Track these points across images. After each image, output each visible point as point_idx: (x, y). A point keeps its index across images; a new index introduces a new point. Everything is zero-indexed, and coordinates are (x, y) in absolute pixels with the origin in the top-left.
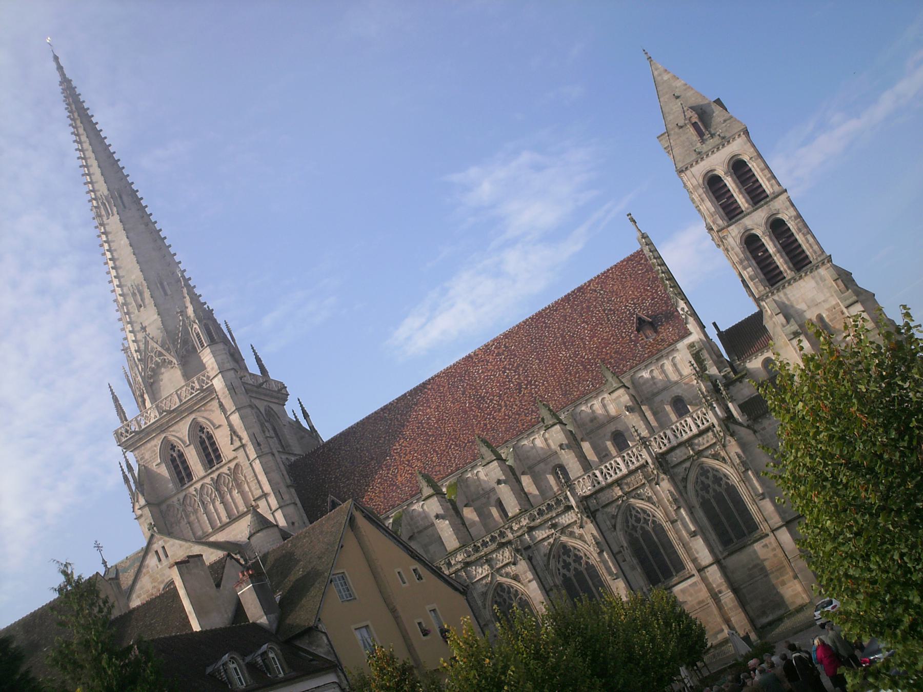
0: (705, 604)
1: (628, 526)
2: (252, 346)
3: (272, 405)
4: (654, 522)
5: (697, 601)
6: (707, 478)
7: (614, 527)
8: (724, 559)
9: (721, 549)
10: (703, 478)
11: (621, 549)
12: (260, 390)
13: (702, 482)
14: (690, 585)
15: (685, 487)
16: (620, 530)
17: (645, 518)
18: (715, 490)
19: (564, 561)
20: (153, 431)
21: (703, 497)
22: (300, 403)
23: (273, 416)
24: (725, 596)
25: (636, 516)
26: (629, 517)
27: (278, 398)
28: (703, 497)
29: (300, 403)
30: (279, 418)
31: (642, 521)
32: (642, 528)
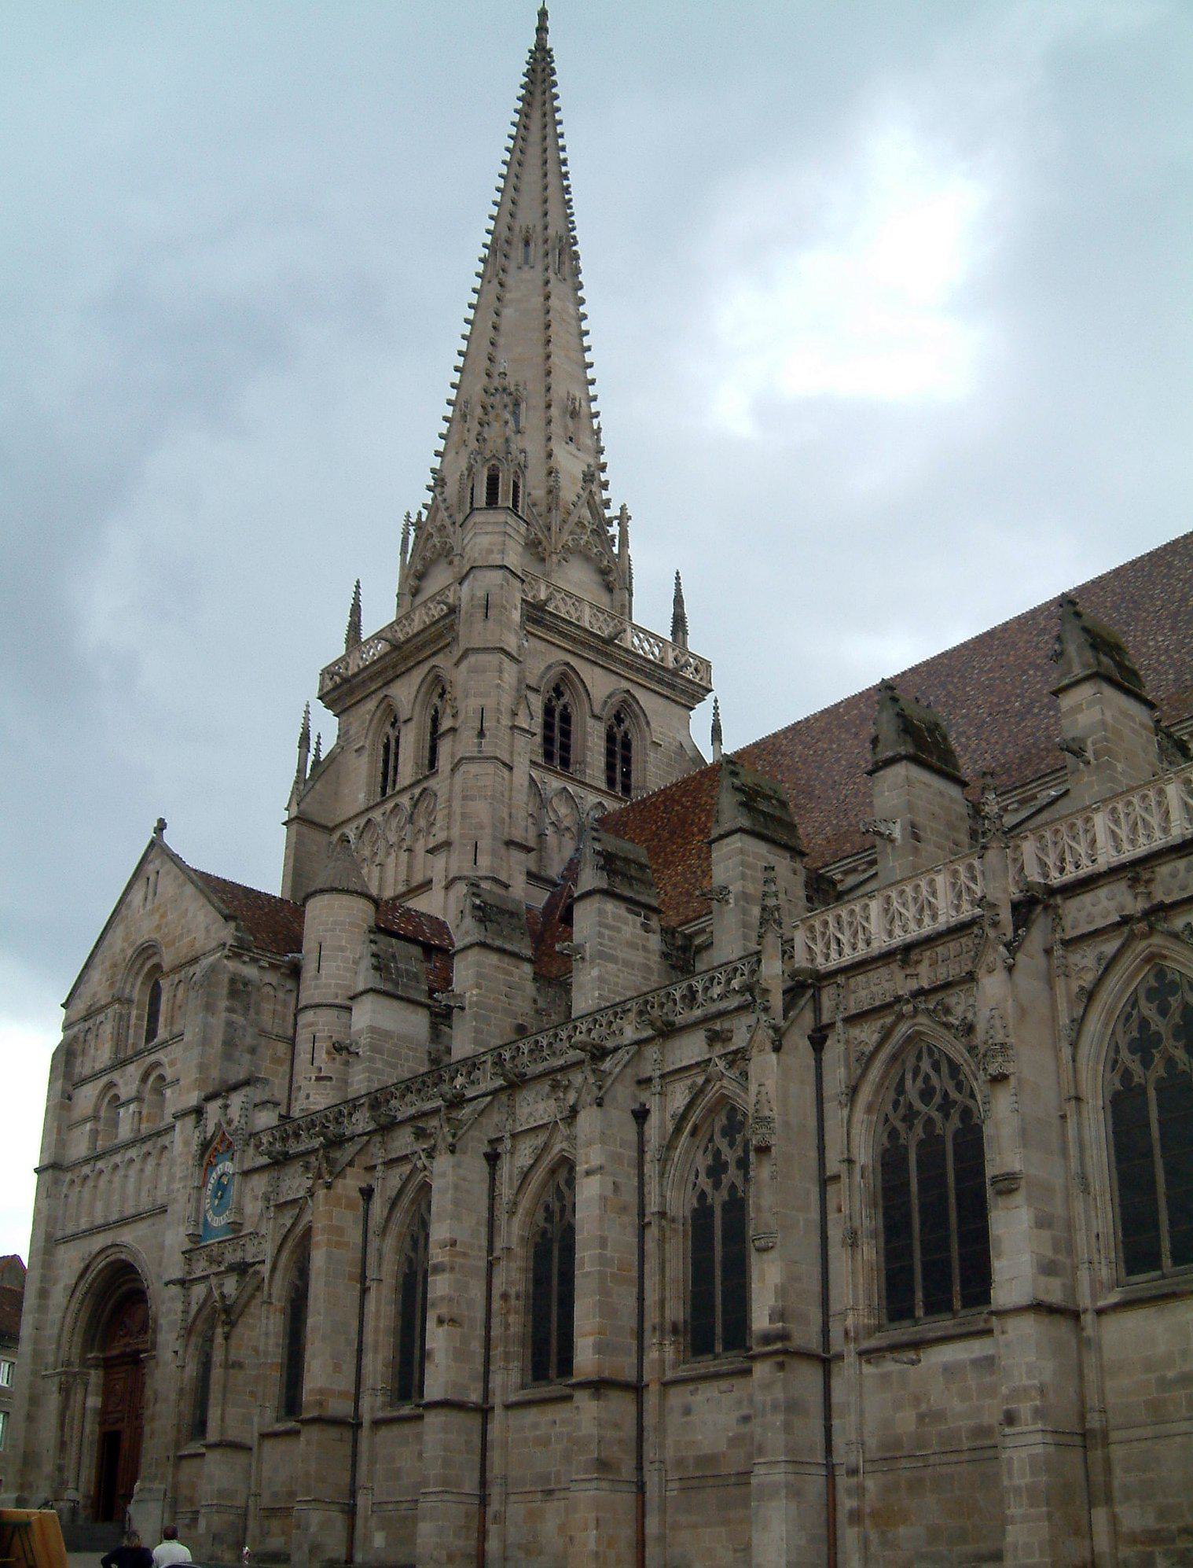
0: (988, 1442)
1: (896, 1104)
2: (678, 573)
3: (639, 693)
4: (966, 1114)
5: (972, 1423)
6: (1163, 1011)
7: (853, 1091)
8: (1100, 1312)
9: (1105, 1273)
10: (1148, 1009)
11: (845, 1166)
12: (610, 649)
13: (1144, 1023)
14: (975, 1362)
15: (1079, 1023)
16: (869, 1109)
17: (946, 1094)
18: (1170, 1062)
19: (717, 1154)
20: (372, 679)
21: (1127, 1075)
22: (716, 708)
23: (637, 717)
24: (1023, 1440)
25: (927, 1078)
26: (909, 1076)
27: (672, 686)
28: (1127, 1075)
29: (716, 708)
30: (648, 723)
31: (938, 1099)
32: (930, 1121)
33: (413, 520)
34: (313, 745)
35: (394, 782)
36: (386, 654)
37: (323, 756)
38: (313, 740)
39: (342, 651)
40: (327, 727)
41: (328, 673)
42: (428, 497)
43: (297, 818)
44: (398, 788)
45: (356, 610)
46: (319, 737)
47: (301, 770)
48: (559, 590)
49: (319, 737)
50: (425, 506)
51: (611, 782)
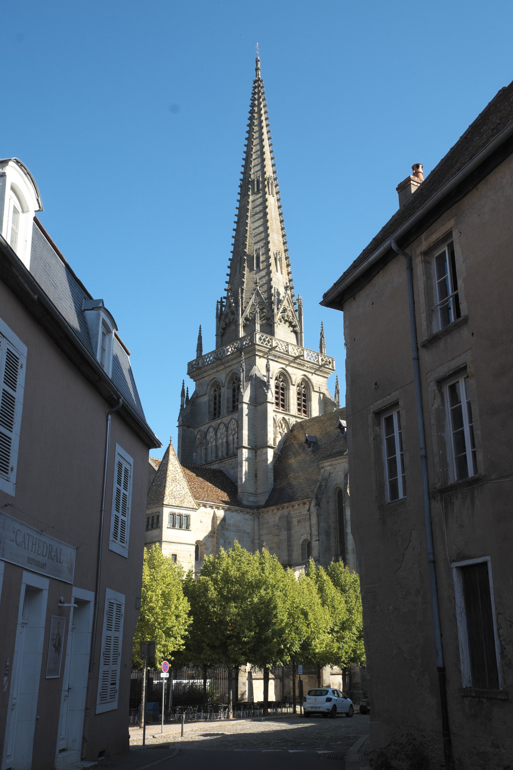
33: (219, 300)
34: (186, 392)
35: (219, 412)
36: (213, 362)
37: (190, 396)
38: (186, 390)
39: (194, 357)
40: (191, 386)
41: (190, 364)
42: (225, 294)
43: (182, 425)
44: (221, 417)
45: (200, 338)
46: (187, 388)
47: (182, 406)
48: (280, 340)
49: (187, 388)
50: (225, 298)
51: (299, 410)
